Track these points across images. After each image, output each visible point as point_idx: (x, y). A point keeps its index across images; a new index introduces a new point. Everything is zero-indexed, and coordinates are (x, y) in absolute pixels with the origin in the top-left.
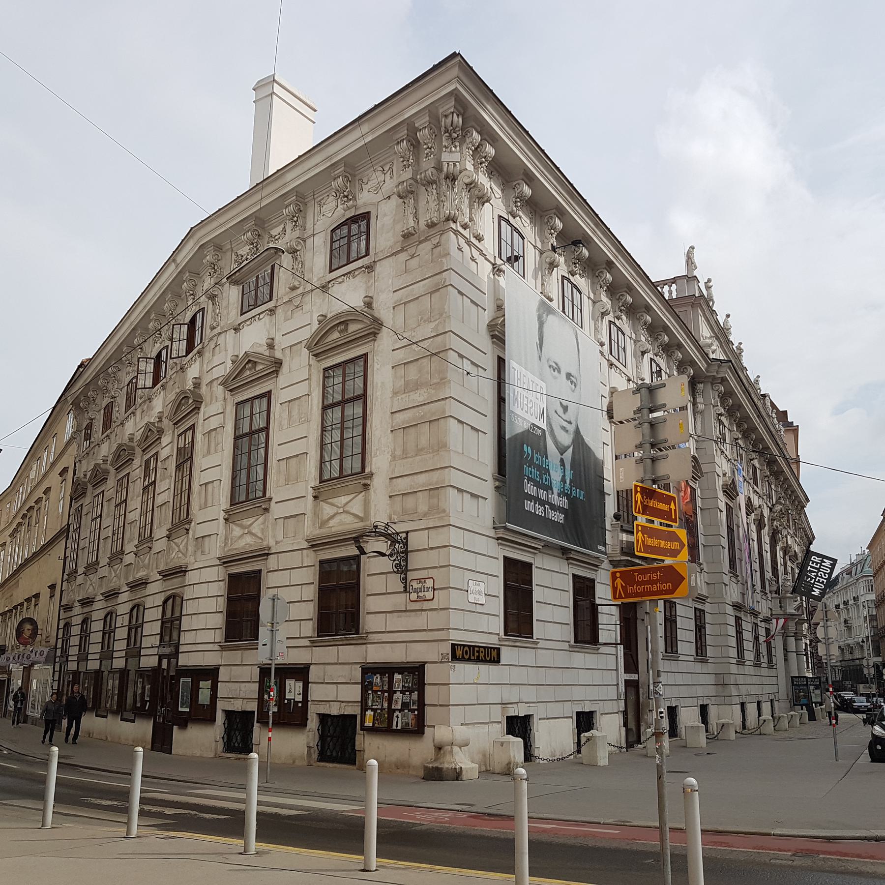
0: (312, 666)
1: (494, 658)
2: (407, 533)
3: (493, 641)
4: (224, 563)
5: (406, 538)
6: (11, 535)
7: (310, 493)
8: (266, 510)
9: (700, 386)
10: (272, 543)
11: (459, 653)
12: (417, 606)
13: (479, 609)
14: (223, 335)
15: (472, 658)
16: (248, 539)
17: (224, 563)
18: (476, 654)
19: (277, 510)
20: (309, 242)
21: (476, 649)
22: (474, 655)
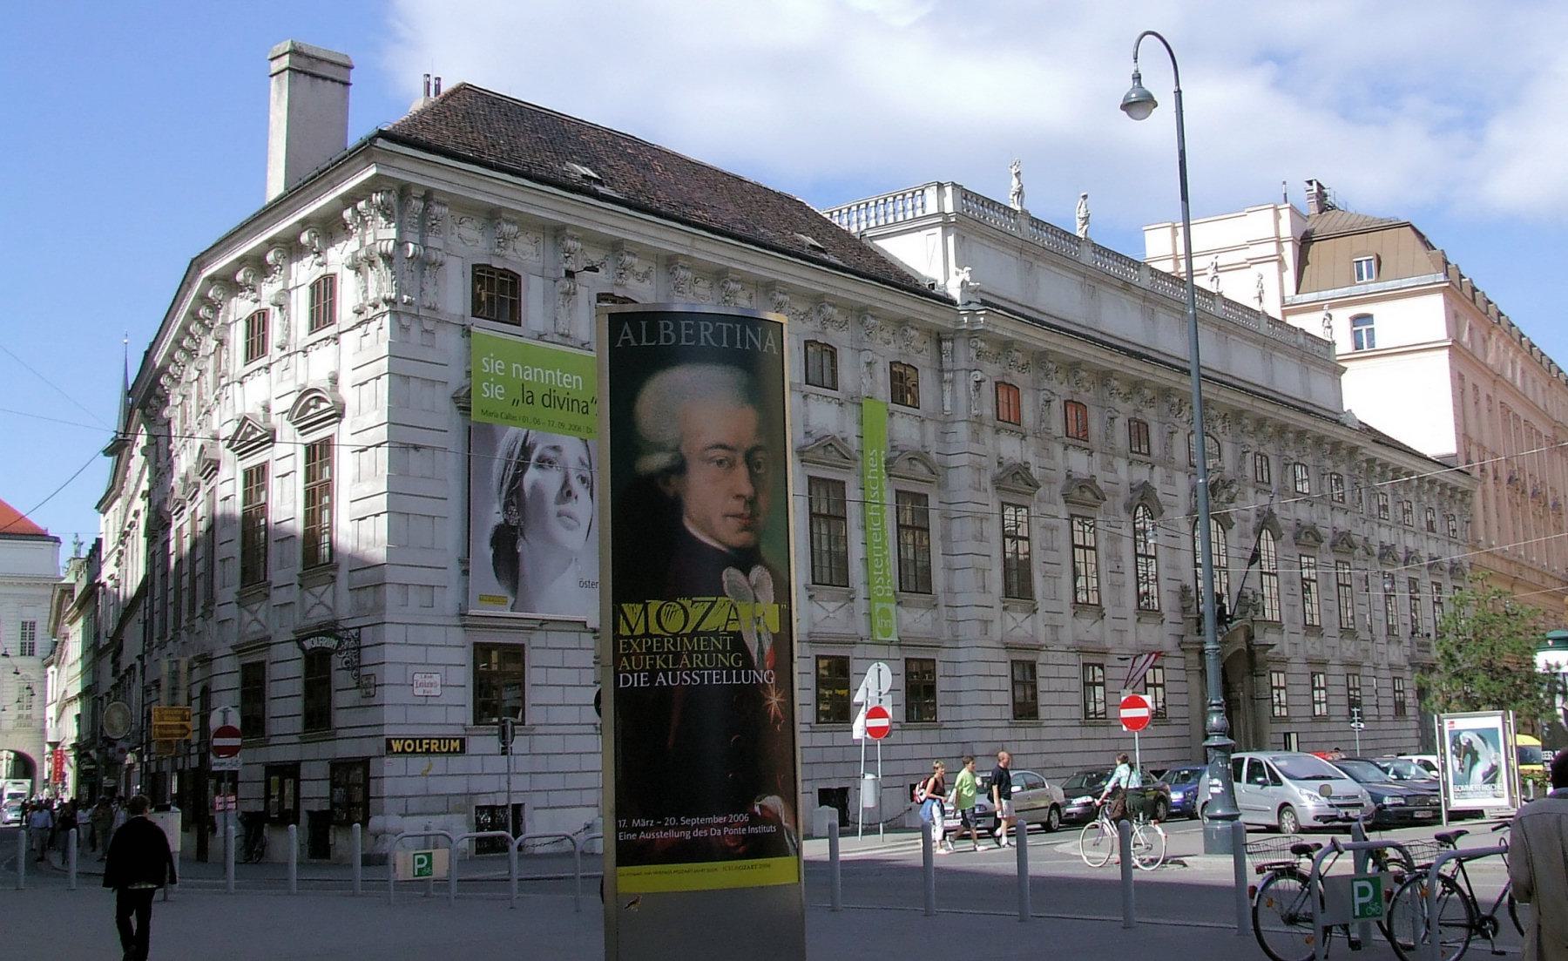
0: (302, 764)
1: (455, 749)
2: (359, 628)
3: (460, 731)
4: (239, 652)
5: (359, 634)
6: (117, 565)
7: (296, 580)
8: (267, 596)
9: (947, 345)
10: (270, 632)
11: (397, 746)
12: (364, 702)
13: (435, 701)
14: (231, 386)
15: (418, 750)
16: (255, 627)
17: (239, 652)
18: (425, 746)
19: (278, 597)
20: (294, 293)
21: (424, 742)
22: (421, 747)
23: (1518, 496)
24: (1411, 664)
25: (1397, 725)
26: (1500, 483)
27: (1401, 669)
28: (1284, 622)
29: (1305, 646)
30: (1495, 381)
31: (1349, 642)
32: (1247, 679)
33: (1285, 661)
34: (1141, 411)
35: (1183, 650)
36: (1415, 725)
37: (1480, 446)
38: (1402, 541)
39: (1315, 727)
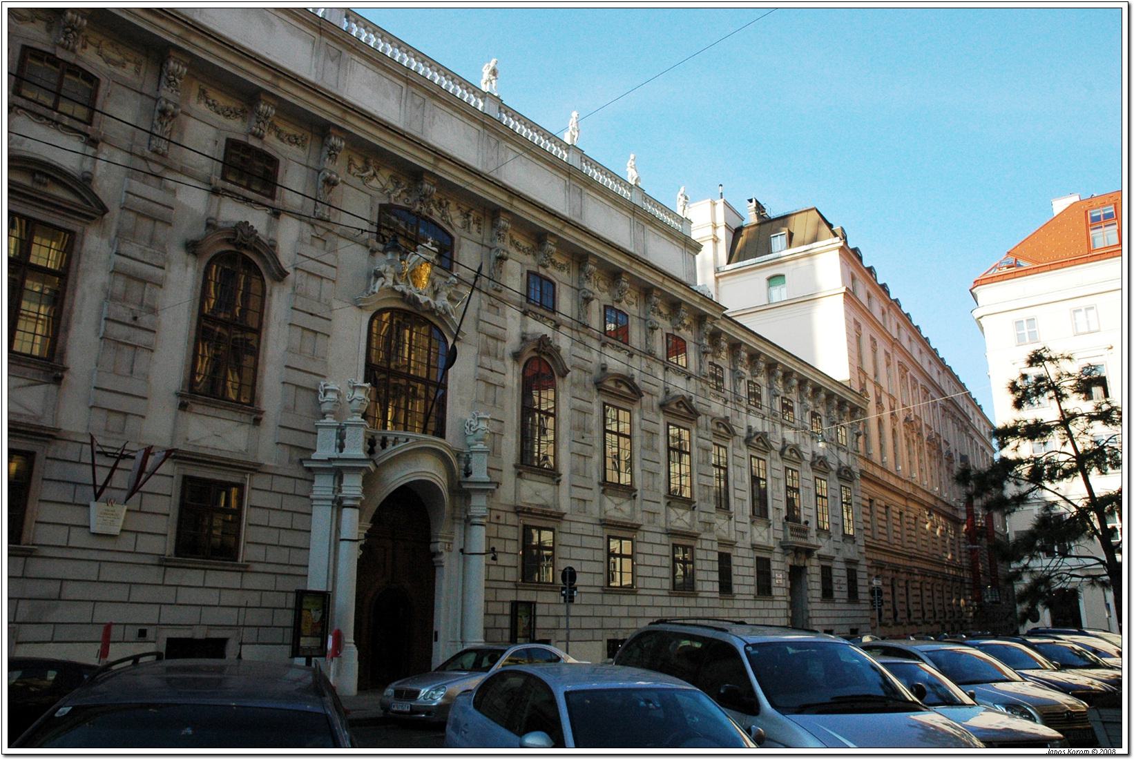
23: (915, 435)
24: (782, 547)
25: (760, 604)
26: (897, 420)
27: (770, 550)
28: (564, 469)
29: (601, 504)
30: (893, 344)
31: (681, 511)
32: (458, 531)
33: (560, 517)
34: (260, 137)
35: (309, 469)
36: (784, 605)
37: (876, 384)
38: (779, 434)
39: (609, 599)
